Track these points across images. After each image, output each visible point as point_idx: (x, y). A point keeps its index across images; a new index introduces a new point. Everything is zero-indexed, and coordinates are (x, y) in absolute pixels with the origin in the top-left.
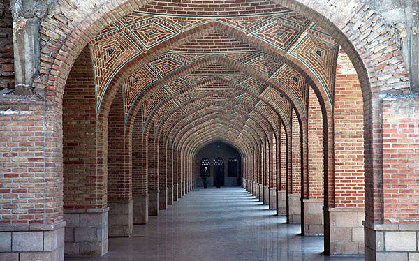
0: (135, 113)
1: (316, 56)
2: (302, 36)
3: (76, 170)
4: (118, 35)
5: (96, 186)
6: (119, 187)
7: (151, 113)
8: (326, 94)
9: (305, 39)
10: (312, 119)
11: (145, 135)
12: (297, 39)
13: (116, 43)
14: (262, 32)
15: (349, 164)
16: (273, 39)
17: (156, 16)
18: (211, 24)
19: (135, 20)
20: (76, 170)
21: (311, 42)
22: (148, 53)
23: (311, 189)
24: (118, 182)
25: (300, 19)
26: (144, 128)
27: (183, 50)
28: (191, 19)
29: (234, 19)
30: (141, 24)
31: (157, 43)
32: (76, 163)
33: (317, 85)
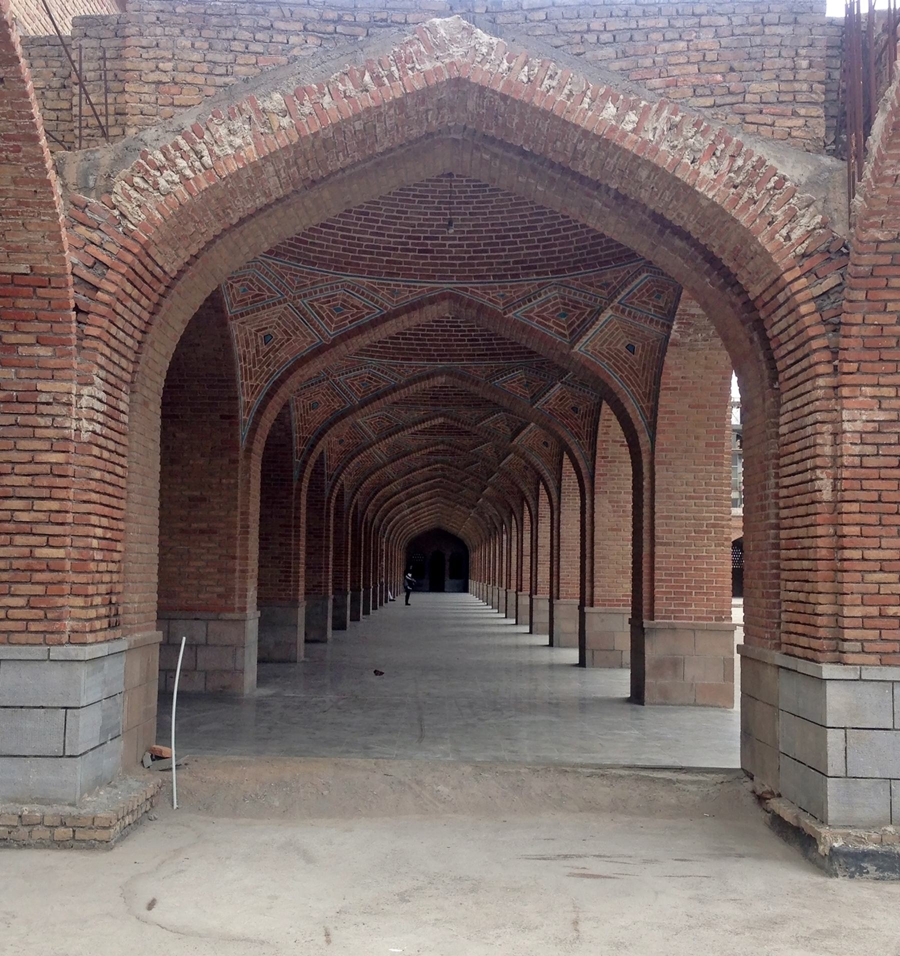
0: (312, 461)
1: (625, 353)
2: (604, 317)
3: (203, 545)
4: (280, 308)
5: (237, 574)
8: (640, 424)
9: (607, 323)
10: (601, 475)
11: (329, 502)
12: (594, 323)
13: (278, 325)
15: (681, 545)
16: (551, 324)
17: (349, 279)
18: (443, 297)
19: (313, 284)
20: (203, 545)
21: (617, 329)
23: (597, 591)
24: (282, 572)
25: (600, 287)
26: (327, 492)
27: (393, 358)
28: (409, 287)
29: (483, 289)
30: (321, 291)
31: (350, 327)
32: (202, 532)
33: (626, 405)
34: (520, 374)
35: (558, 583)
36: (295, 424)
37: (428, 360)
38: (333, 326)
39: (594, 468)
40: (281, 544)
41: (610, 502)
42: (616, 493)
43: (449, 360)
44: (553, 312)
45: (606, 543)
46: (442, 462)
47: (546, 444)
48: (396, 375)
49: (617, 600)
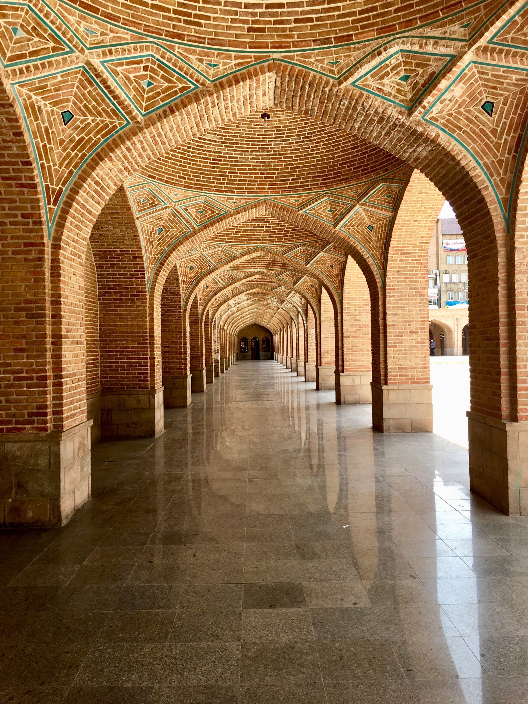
7: (74, 179)
46: (262, 249)
47: (488, 108)
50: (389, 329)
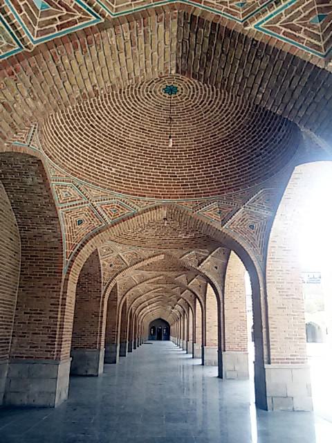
6: (49, 344)
10: (271, 270)
11: (104, 298)
14: (279, 18)
22: (35, 53)
24: (49, 337)
26: (103, 292)
27: (134, 195)
34: (215, 205)
35: (224, 342)
36: (64, 234)
37: (156, 197)
38: (37, 28)
39: (265, 266)
40: (50, 317)
41: (277, 289)
42: (281, 283)
43: (169, 198)
44: (301, 20)
45: (276, 317)
47: (216, 268)
48: (135, 206)
49: (287, 359)
50: (207, 324)
